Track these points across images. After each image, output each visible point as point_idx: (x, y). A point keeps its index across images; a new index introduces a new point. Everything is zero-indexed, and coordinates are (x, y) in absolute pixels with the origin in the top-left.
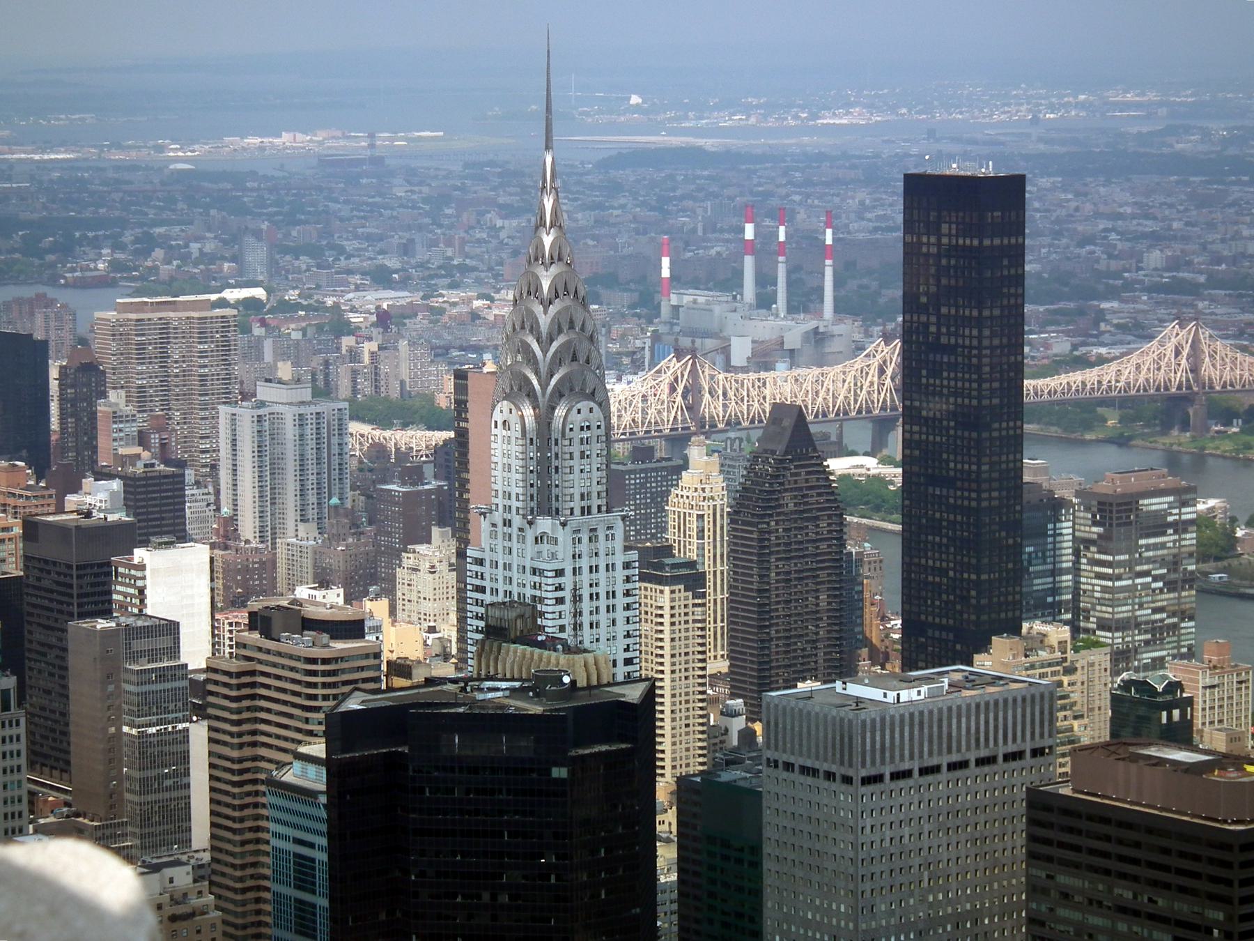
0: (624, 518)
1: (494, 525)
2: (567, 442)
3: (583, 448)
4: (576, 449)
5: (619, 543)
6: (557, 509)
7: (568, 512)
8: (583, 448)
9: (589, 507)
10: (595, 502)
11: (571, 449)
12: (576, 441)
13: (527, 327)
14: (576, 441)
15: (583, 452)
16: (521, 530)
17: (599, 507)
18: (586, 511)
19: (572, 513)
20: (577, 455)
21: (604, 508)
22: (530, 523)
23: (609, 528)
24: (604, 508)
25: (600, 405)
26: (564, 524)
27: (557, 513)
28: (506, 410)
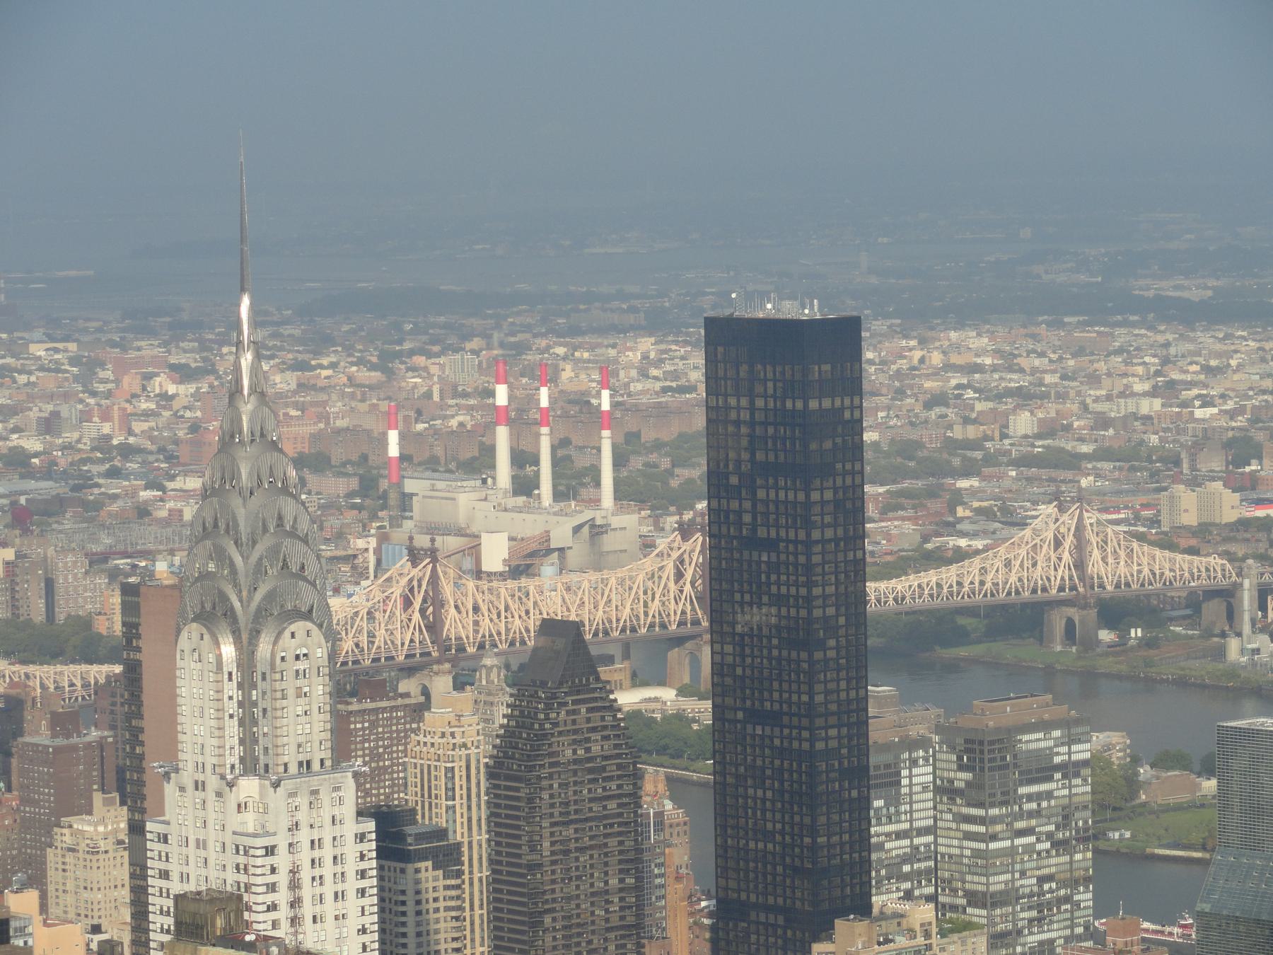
0: (356, 775)
2: (278, 676)
5: (349, 810)
6: (267, 766)
7: (281, 769)
8: (299, 683)
9: (308, 763)
11: (284, 685)
12: (289, 675)
13: (222, 525)
17: (322, 761)
19: (286, 771)
20: (291, 693)
21: (328, 763)
22: (231, 785)
23: (337, 789)
24: (328, 763)
25: (320, 626)
26: (276, 785)
27: (267, 771)
28: (195, 636)
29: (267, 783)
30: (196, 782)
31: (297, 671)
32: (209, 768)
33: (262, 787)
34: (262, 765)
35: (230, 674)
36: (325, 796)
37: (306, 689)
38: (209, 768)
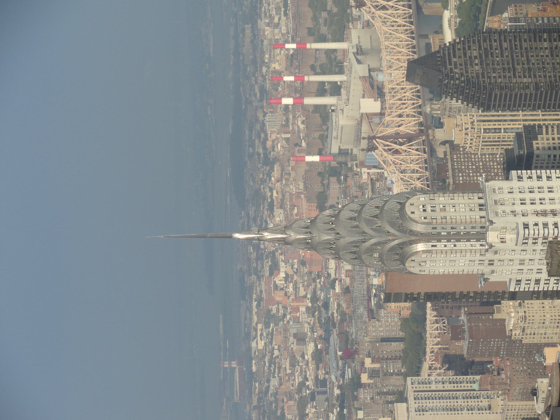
0: (487, 180)
2: (434, 221)
3: (438, 210)
5: (505, 185)
6: (481, 227)
7: (483, 220)
8: (438, 210)
9: (480, 205)
11: (439, 218)
12: (434, 215)
13: (355, 249)
16: (496, 253)
17: (479, 198)
19: (484, 217)
20: (443, 214)
21: (480, 195)
22: (491, 246)
23: (494, 191)
24: (480, 195)
25: (408, 198)
26: (492, 223)
27: (484, 227)
28: (412, 264)
29: (490, 227)
30: (489, 264)
31: (432, 211)
32: (482, 258)
33: (492, 230)
34: (481, 230)
35: (433, 246)
36: (498, 197)
37: (441, 206)
38: (482, 258)
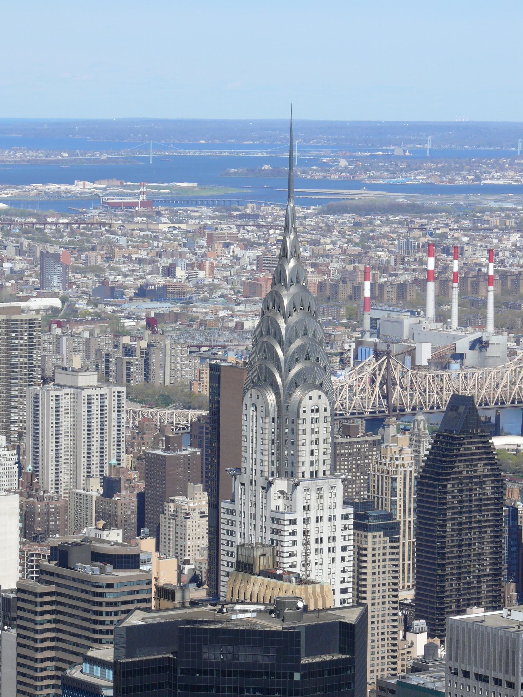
0: (343, 481)
1: (243, 484)
2: (301, 421)
3: (312, 426)
4: (308, 426)
7: (300, 475)
8: (312, 426)
9: (317, 472)
10: (321, 468)
11: (304, 427)
12: (308, 421)
13: (272, 332)
14: (308, 421)
15: (313, 429)
17: (324, 472)
18: (314, 474)
19: (303, 476)
20: (308, 431)
21: (328, 473)
23: (332, 488)
24: (328, 473)
25: (326, 393)
27: (292, 476)
28: (254, 396)
31: (312, 419)
35: (273, 419)
36: (326, 492)
37: (317, 430)
